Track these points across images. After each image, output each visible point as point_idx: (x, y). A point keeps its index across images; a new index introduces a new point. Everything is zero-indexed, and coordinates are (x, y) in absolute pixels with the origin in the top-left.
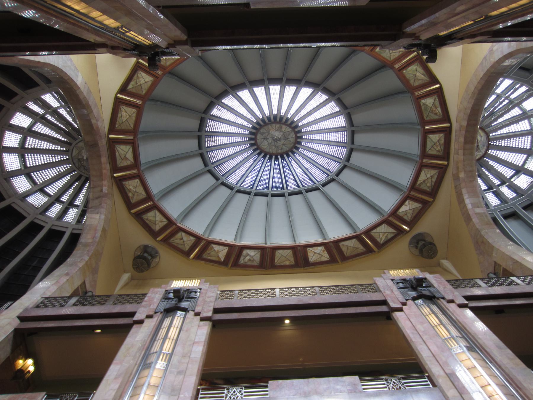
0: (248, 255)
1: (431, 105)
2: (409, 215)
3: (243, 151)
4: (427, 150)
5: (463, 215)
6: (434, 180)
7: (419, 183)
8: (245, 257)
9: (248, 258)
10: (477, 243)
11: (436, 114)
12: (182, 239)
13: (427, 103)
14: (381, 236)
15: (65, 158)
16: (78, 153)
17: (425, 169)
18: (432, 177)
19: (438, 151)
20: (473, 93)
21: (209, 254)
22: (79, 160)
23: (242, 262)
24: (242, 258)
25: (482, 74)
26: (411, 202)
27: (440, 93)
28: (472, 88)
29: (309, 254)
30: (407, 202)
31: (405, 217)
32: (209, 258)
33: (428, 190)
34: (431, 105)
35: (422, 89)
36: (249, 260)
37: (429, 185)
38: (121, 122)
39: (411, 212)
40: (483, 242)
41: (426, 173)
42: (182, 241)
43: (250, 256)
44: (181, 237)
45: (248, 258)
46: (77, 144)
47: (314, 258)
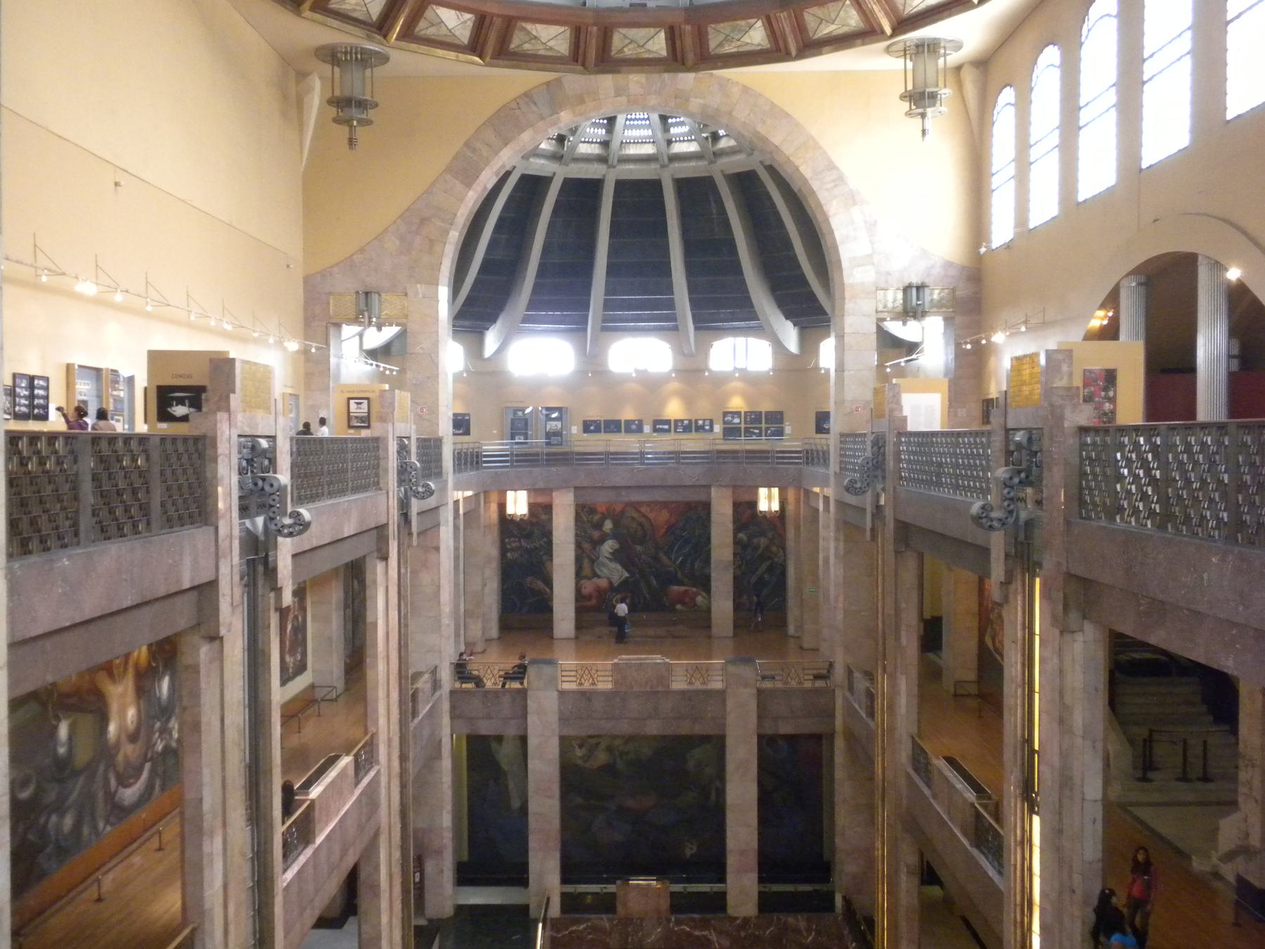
1: (746, 39)
4: (624, 31)
5: (467, 144)
6: (542, 52)
7: (529, 26)
10: (423, 221)
11: (721, 45)
13: (752, 32)
17: (568, 32)
18: (551, 49)
19: (621, 51)
20: (765, 140)
25: (806, 171)
26: (470, 24)
27: (776, 52)
28: (776, 139)
30: (468, 16)
31: (422, 24)
33: (512, 46)
34: (746, 39)
37: (527, 46)
39: (443, 31)
40: (432, 242)
41: (562, 36)
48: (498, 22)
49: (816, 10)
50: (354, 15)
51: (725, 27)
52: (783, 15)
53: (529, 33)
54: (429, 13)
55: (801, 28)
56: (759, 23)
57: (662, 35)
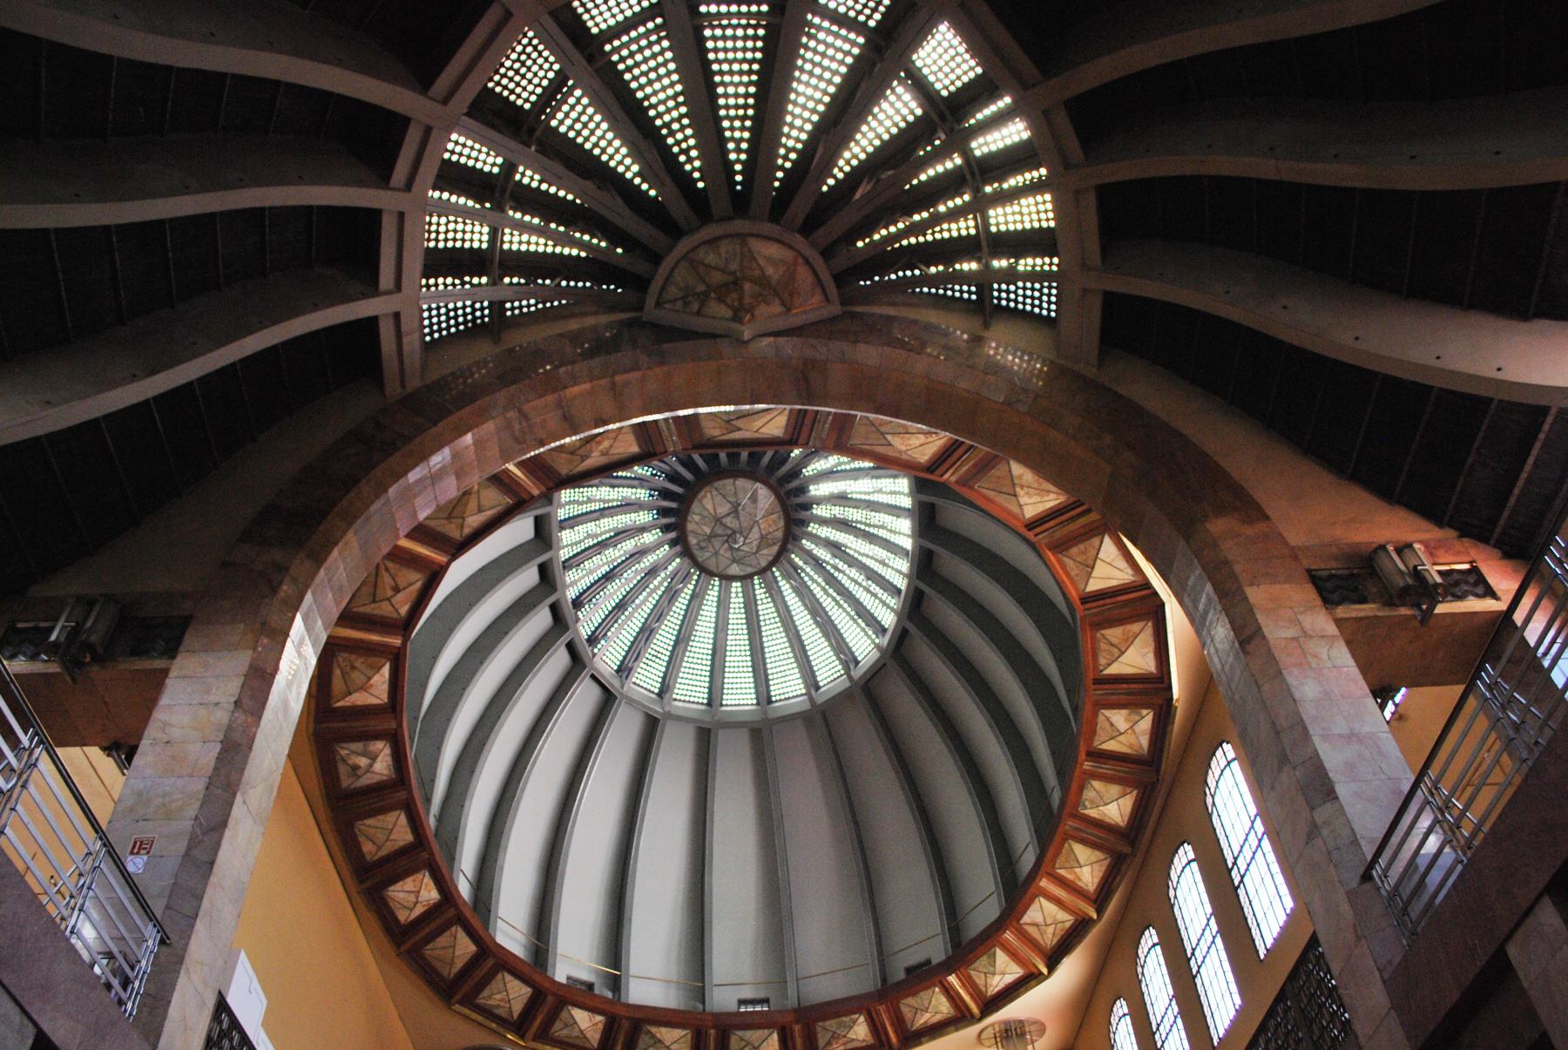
0: (374, 758)
1: (851, 1035)
2: (565, 1032)
3: (723, 605)
4: (740, 1033)
7: (654, 1030)
8: (365, 754)
9: (363, 762)
12: (397, 590)
13: (856, 1028)
14: (498, 997)
15: (733, 156)
16: (763, 281)
21: (353, 668)
22: (735, 284)
23: (344, 752)
24: (355, 746)
26: (601, 1026)
29: (409, 880)
30: (599, 1018)
31: (558, 1025)
32: (338, 672)
34: (851, 1035)
35: (892, 1025)
36: (355, 768)
38: (883, 429)
39: (576, 1033)
42: (390, 593)
43: (371, 766)
44: (402, 583)
45: (363, 762)
46: (807, 262)
47: (402, 895)
48: (626, 1024)
49: (910, 1001)
50: (497, 1011)
51: (831, 1024)
52: (882, 1008)
53: (653, 1036)
54: (564, 1014)
55: (899, 1021)
56: (862, 1019)
57: (775, 1036)
